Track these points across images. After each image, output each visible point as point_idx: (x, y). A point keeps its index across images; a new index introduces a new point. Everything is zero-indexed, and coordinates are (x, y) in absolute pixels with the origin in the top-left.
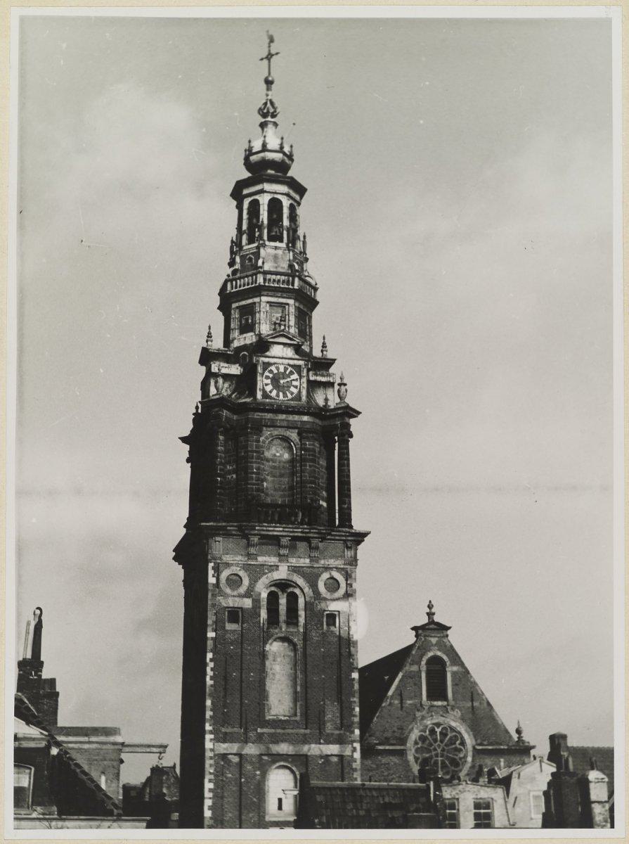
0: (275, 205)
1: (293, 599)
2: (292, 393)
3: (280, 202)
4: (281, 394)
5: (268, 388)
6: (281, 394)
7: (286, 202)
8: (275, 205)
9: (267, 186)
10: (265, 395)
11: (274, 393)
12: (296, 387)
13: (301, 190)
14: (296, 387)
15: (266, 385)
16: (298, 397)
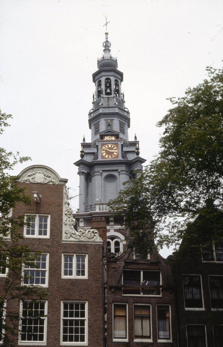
0: (108, 81)
1: (117, 244)
2: (114, 155)
3: (109, 79)
4: (110, 156)
5: (104, 154)
6: (110, 156)
7: (113, 79)
8: (108, 81)
9: (103, 74)
10: (103, 157)
11: (107, 156)
12: (116, 152)
13: (121, 74)
14: (116, 152)
15: (103, 153)
16: (117, 156)
